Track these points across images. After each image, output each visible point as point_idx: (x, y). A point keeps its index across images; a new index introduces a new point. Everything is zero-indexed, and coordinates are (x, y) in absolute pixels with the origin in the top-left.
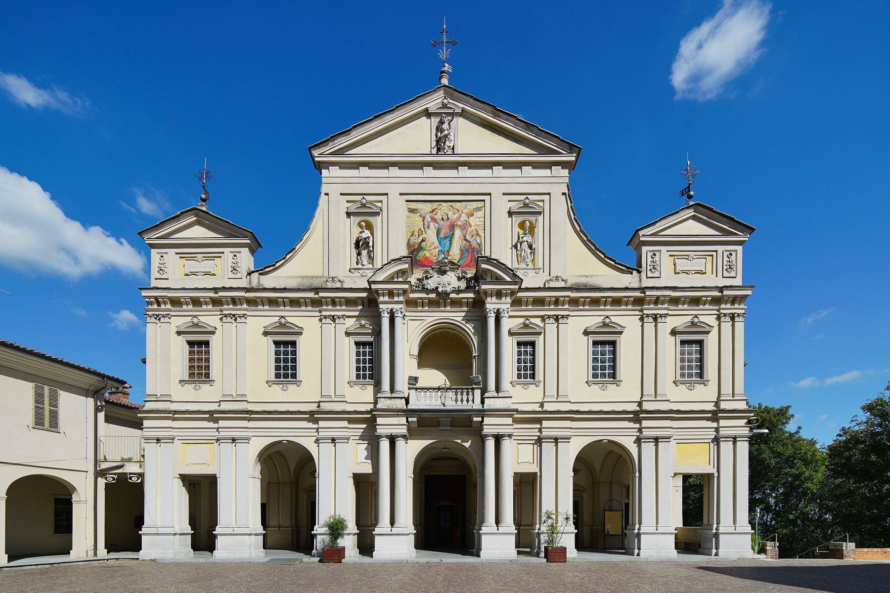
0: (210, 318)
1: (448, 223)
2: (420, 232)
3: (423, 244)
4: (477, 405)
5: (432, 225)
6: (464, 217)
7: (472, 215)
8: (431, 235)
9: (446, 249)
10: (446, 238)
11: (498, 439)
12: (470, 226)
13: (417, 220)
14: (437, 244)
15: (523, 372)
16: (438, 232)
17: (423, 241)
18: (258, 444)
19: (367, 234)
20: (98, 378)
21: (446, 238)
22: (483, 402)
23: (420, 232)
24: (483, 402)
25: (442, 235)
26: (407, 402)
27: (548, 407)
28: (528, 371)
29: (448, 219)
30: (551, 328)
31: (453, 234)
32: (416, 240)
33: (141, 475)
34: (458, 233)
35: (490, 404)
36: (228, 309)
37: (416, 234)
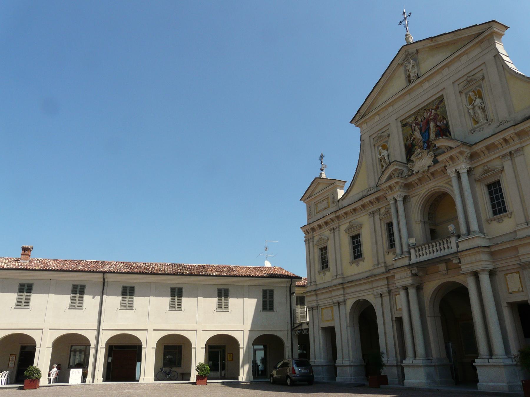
0: (326, 232)
1: (425, 121)
2: (411, 136)
3: (414, 142)
4: (454, 249)
5: (417, 128)
6: (433, 111)
7: (437, 108)
8: (417, 134)
9: (427, 139)
10: (425, 132)
11: (476, 275)
12: (438, 115)
13: (408, 128)
14: (421, 138)
15: (497, 208)
16: (421, 129)
17: (413, 140)
18: (350, 303)
19: (385, 153)
20: (287, 279)
21: (425, 132)
22: (458, 247)
23: (411, 136)
24: (458, 247)
25: (423, 131)
26: (410, 259)
27: (521, 234)
28: (499, 206)
29: (425, 118)
30: (507, 164)
31: (429, 127)
32: (409, 143)
33: (308, 330)
34: (432, 124)
35: (462, 247)
36: (331, 226)
37: (409, 138)
